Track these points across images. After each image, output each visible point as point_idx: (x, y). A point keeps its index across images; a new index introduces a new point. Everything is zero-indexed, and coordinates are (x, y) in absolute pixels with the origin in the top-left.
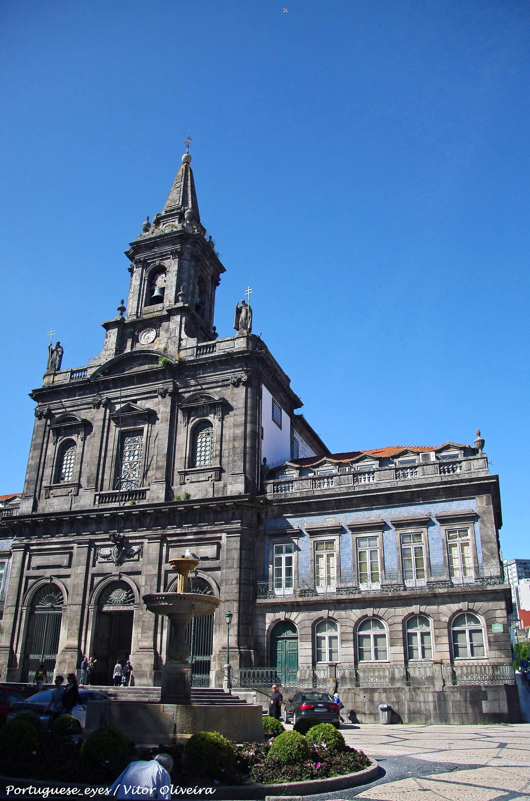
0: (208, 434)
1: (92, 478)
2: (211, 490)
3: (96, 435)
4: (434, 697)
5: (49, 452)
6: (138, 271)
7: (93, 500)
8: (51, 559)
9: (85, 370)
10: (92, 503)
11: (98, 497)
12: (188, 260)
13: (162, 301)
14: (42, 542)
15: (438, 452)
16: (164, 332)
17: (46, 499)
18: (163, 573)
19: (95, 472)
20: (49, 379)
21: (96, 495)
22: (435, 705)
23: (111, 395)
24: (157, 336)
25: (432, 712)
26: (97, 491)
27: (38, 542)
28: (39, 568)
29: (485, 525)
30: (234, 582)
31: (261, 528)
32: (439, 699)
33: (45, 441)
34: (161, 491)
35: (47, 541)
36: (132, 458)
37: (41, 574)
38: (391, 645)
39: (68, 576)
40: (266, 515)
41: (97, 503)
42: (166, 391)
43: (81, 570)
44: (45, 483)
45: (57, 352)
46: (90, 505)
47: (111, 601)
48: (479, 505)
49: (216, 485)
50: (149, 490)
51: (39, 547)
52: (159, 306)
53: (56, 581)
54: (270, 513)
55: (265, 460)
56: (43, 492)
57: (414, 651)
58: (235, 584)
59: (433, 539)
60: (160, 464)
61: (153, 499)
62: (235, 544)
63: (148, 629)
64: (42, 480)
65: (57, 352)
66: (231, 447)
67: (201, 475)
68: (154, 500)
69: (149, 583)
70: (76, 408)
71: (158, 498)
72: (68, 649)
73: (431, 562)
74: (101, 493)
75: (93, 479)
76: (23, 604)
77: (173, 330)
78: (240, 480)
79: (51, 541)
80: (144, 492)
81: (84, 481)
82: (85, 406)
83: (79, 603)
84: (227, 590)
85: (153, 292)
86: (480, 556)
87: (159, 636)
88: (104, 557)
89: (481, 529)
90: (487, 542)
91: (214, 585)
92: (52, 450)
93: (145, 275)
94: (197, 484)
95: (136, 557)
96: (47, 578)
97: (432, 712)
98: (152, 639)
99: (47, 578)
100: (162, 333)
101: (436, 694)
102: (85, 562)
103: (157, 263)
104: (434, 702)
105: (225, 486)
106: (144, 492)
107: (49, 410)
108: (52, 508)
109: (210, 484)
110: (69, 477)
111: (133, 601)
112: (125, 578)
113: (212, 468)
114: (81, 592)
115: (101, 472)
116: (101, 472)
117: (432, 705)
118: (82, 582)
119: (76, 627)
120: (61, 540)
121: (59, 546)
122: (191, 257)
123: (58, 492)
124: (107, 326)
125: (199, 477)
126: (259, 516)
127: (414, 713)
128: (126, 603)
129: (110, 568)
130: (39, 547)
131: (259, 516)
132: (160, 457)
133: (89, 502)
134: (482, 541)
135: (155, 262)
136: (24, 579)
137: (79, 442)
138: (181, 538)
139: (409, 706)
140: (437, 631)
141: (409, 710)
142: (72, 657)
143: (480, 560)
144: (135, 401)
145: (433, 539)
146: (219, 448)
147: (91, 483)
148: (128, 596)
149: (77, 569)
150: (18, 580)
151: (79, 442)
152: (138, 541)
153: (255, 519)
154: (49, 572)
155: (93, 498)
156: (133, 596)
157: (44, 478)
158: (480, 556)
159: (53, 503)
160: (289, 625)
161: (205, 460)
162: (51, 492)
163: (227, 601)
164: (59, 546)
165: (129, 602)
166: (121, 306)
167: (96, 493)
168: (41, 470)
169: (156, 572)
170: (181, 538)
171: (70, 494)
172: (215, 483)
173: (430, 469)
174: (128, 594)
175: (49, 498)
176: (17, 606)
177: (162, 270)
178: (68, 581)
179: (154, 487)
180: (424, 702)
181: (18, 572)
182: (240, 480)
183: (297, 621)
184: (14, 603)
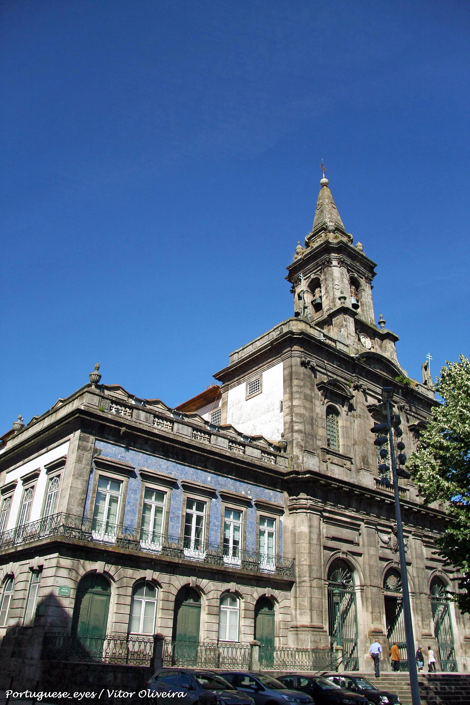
8: (344, 532)
14: (336, 511)
17: (323, 461)
27: (332, 510)
28: (334, 539)
35: (340, 512)
37: (338, 547)
39: (360, 555)
51: (331, 516)
53: (350, 557)
57: (176, 594)
79: (343, 513)
120: (353, 515)
121: (349, 520)
130: (331, 516)
154: (345, 547)
164: (349, 520)
178: (360, 559)
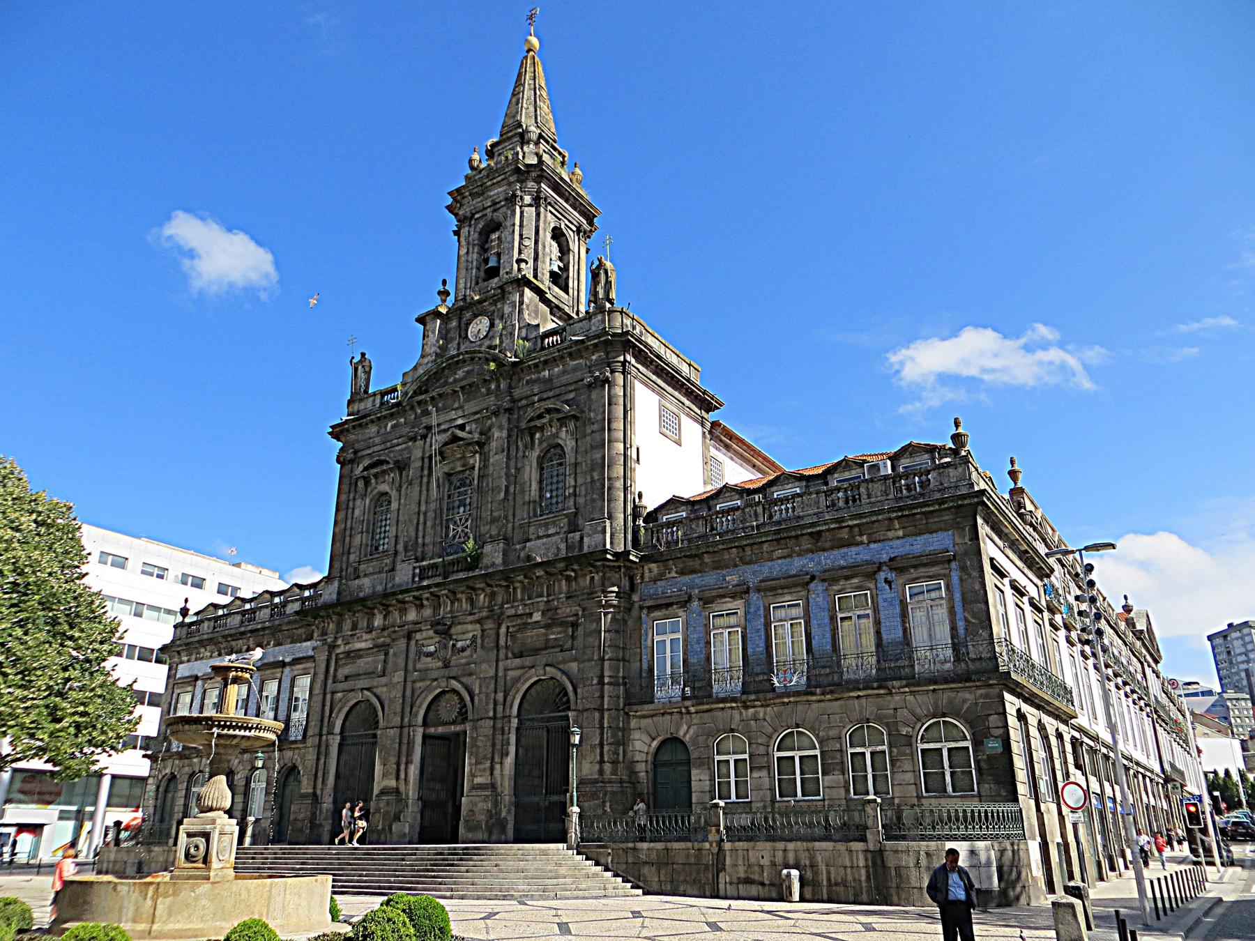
2: (563, 546)
4: (866, 860)
5: (357, 512)
6: (464, 231)
11: (417, 571)
13: (498, 275)
15: (894, 458)
18: (501, 673)
19: (413, 534)
22: (868, 872)
24: (492, 325)
25: (864, 884)
26: (417, 560)
28: (347, 678)
29: (969, 575)
30: (595, 682)
31: (635, 598)
32: (874, 863)
36: (462, 509)
38: (823, 774)
40: (642, 577)
42: (499, 408)
43: (398, 677)
44: (352, 557)
45: (362, 367)
48: (958, 540)
52: (494, 282)
54: (647, 574)
55: (640, 495)
59: (885, 600)
60: (495, 514)
63: (485, 758)
64: (349, 553)
65: (362, 367)
66: (589, 480)
69: (484, 690)
71: (493, 564)
72: (384, 792)
73: (885, 637)
81: (400, 547)
84: (586, 695)
85: (486, 261)
86: (961, 625)
87: (498, 767)
88: (429, 655)
89: (961, 580)
90: (971, 602)
91: (570, 688)
92: (361, 508)
93: (475, 236)
95: (468, 653)
97: (864, 884)
98: (488, 772)
100: (497, 322)
101: (869, 856)
102: (403, 665)
104: (867, 867)
105: (582, 538)
107: (355, 453)
110: (386, 545)
111: (466, 718)
114: (399, 709)
115: (421, 534)
116: (421, 534)
117: (863, 872)
118: (400, 695)
119: (393, 760)
125: (547, 529)
126: (632, 579)
127: (837, 884)
131: (632, 579)
132: (495, 505)
134: (964, 599)
136: (329, 696)
137: (394, 494)
139: (829, 873)
140: (895, 750)
141: (829, 880)
142: (388, 803)
143: (961, 631)
144: (462, 427)
145: (885, 600)
146: (573, 483)
151: (394, 494)
153: (625, 582)
156: (466, 712)
158: (961, 625)
160: (674, 741)
161: (557, 503)
162: (362, 567)
163: (587, 710)
166: (441, 288)
168: (347, 539)
169: (492, 673)
173: (877, 488)
175: (358, 577)
176: (321, 735)
177: (496, 226)
180: (852, 867)
183: (687, 738)
184: (317, 731)
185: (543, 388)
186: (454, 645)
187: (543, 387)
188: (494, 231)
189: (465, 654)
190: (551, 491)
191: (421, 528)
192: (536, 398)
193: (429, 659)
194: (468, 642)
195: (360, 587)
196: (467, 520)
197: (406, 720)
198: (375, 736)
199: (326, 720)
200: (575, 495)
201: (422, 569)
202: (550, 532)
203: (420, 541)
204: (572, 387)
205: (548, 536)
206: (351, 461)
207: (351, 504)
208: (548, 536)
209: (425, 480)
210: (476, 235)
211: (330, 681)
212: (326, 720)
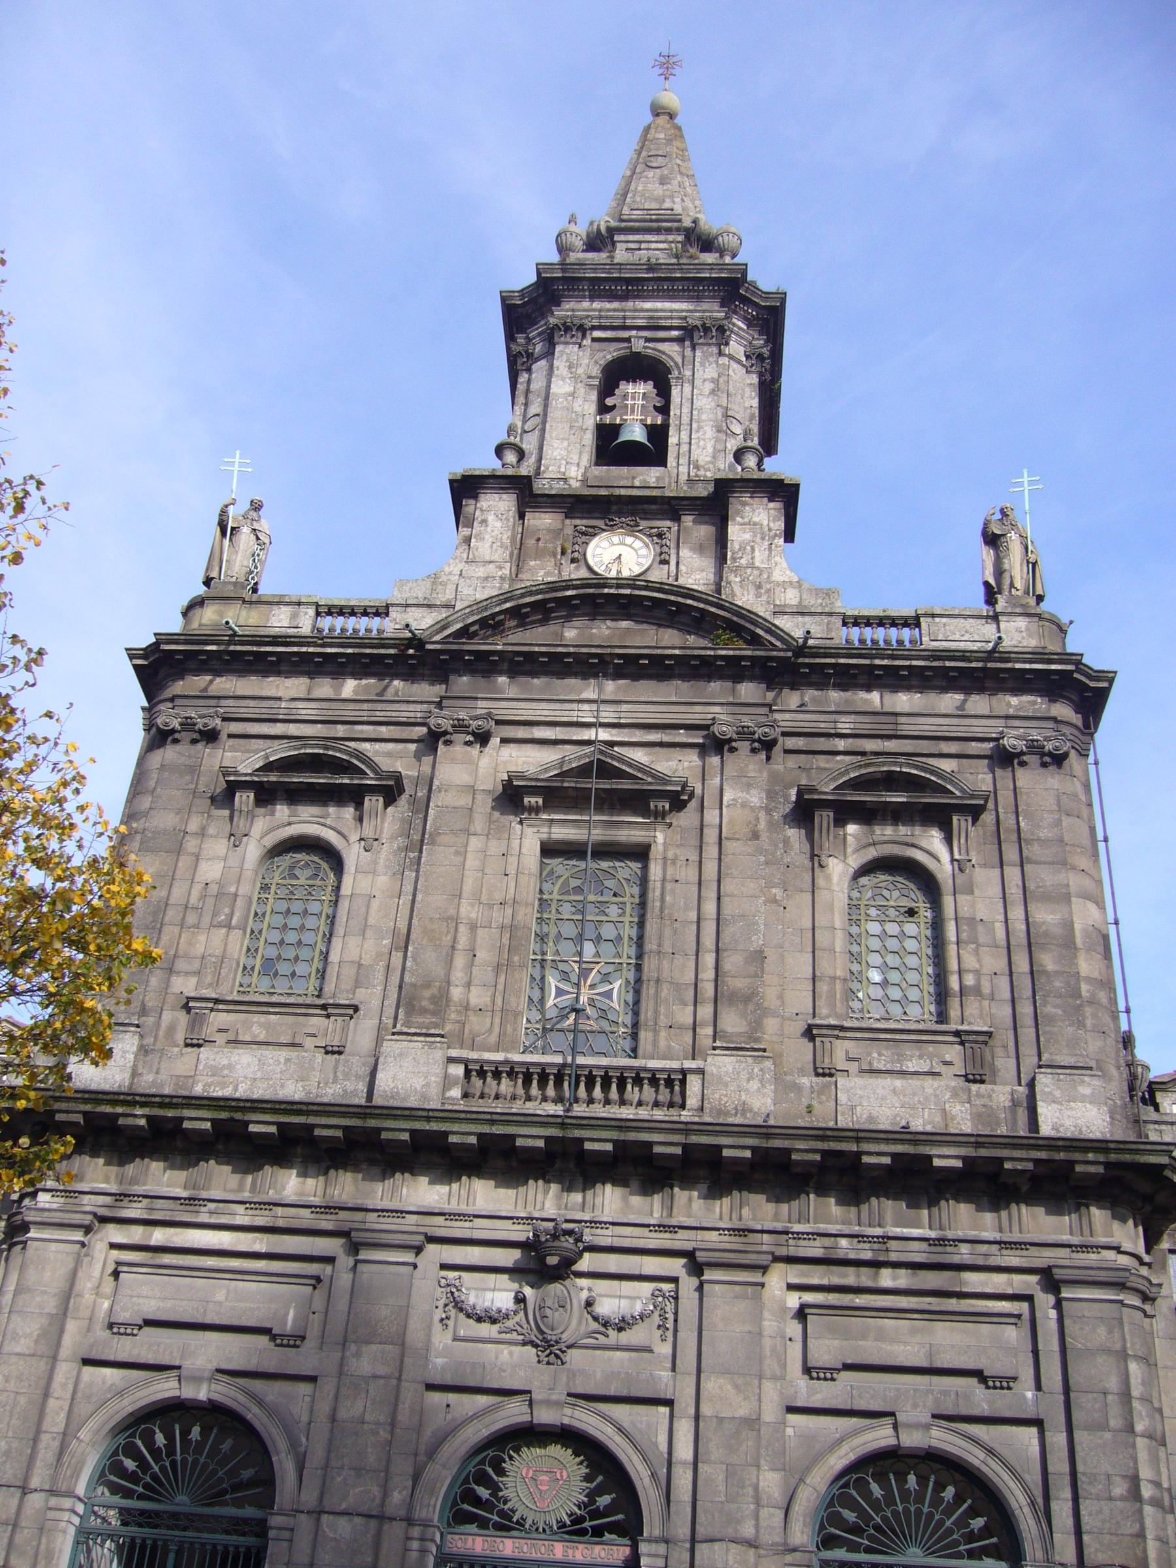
0: (911, 912)
1: (427, 994)
3: (440, 839)
5: (211, 871)
7: (435, 1079)
8: (220, 1296)
9: (382, 611)
10: (434, 1090)
11: (458, 1071)
12: (739, 362)
16: (691, 549)
19: (440, 971)
20: (221, 614)
21: (451, 1060)
23: (504, 710)
33: (193, 827)
34: (754, 1085)
41: (456, 1093)
46: (424, 1097)
47: (502, 1514)
49: (979, 1095)
50: (701, 1072)
51: (159, 1236)
52: (647, 477)
56: (175, 1018)
58: (1122, 1498)
61: (719, 1112)
62: (1102, 1331)
64: (171, 971)
67: (908, 1050)
68: (727, 1114)
70: (341, 731)
71: (744, 1109)
74: (474, 1055)
75: (434, 1000)
76: (54, 1478)
77: (742, 548)
78: (1087, 1091)
80: (675, 1082)
82: (384, 731)
83: (364, 1509)
94: (898, 1083)
96: (197, 1379)
99: (197, 1379)
103: (638, 346)
106: (675, 1082)
108: (223, 1085)
109: (955, 1094)
112: (586, 1420)
113: (957, 1033)
114: (373, 1458)
116: (458, 975)
121: (259, 1242)
122: (747, 357)
123: (257, 1026)
124: (466, 488)
125: (901, 1058)
128: (582, 1532)
129: (511, 1361)
130: (159, 1236)
133: (418, 1083)
135: (628, 340)
136: (65, 1370)
137: (352, 855)
138: (849, 1277)
147: (424, 1011)
148: (592, 1501)
149: (358, 1355)
150: (42, 1366)
152: (651, 1265)
155: (438, 1069)
157: (181, 965)
159: (230, 1067)
165: (598, 1532)
167: (454, 1053)
170: (849, 1277)
171: (309, 1043)
172: (974, 1087)
174: (592, 1495)
176: (25, 1490)
179: (721, 1064)
181: (44, 1334)
182: (1085, 1090)
185: (864, 729)
186: (589, 1304)
187: (865, 724)
188: (633, 378)
189: (625, 1338)
190: (884, 968)
191: (460, 961)
192: (841, 745)
193: (487, 1330)
194: (638, 1308)
195: (215, 1071)
196: (606, 978)
197: (397, 1497)
198: (261, 1529)
199: (48, 1446)
200: (977, 990)
201: (476, 1071)
202: (911, 1066)
203: (456, 993)
204: (953, 748)
205: (902, 1073)
206: (210, 736)
207: (191, 844)
208: (902, 1073)
209: (475, 843)
210: (596, 371)
211: (71, 1326)
212: (48, 1446)
